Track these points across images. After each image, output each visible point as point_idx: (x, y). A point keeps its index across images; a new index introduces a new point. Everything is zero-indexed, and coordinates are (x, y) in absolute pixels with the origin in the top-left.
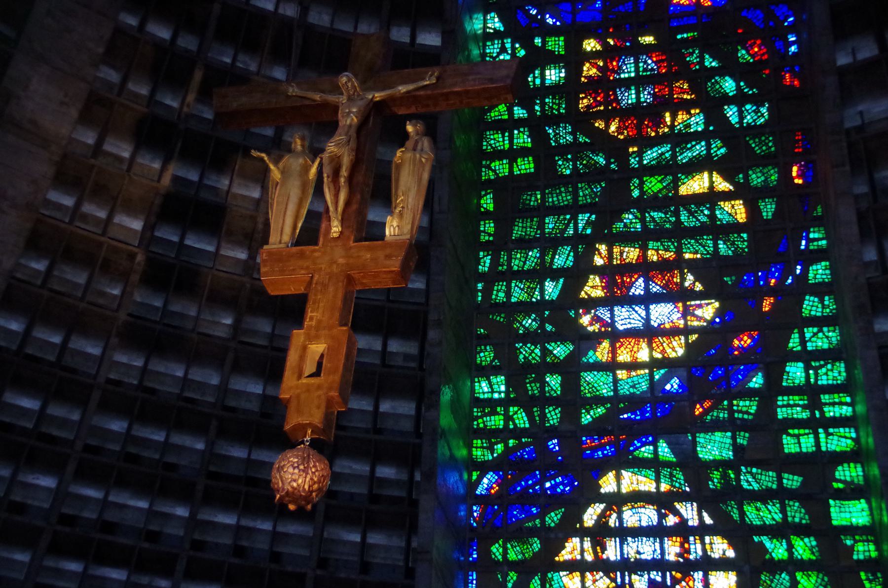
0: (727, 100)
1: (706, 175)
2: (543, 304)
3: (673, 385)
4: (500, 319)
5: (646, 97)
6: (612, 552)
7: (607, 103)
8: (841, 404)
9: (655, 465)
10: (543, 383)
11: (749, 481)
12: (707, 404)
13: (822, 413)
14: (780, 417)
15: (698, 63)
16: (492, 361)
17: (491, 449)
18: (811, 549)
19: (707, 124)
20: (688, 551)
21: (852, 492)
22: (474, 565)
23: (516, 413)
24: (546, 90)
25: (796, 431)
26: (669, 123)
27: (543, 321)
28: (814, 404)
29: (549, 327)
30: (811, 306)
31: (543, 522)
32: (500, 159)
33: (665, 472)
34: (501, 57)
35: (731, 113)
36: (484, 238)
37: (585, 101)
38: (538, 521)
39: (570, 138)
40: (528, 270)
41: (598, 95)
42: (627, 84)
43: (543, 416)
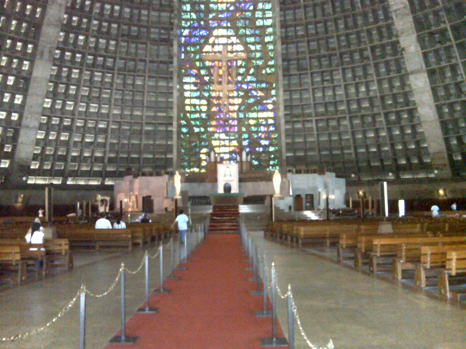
3: (232, 8)
9: (227, 28)
10: (200, 7)
12: (240, 13)
21: (270, 35)
22: (183, 52)
33: (229, 30)
43: (200, 16)
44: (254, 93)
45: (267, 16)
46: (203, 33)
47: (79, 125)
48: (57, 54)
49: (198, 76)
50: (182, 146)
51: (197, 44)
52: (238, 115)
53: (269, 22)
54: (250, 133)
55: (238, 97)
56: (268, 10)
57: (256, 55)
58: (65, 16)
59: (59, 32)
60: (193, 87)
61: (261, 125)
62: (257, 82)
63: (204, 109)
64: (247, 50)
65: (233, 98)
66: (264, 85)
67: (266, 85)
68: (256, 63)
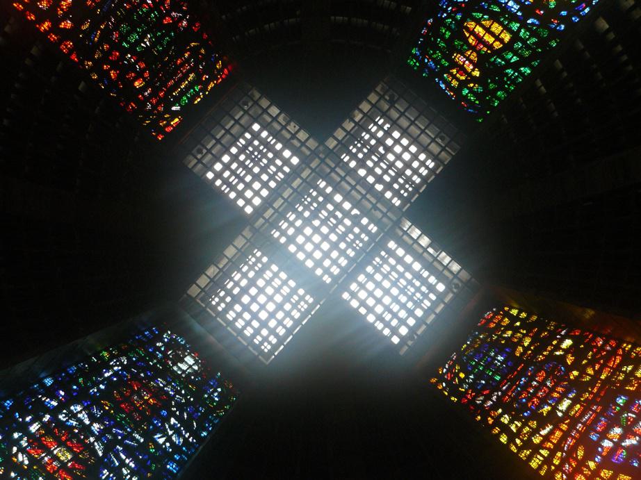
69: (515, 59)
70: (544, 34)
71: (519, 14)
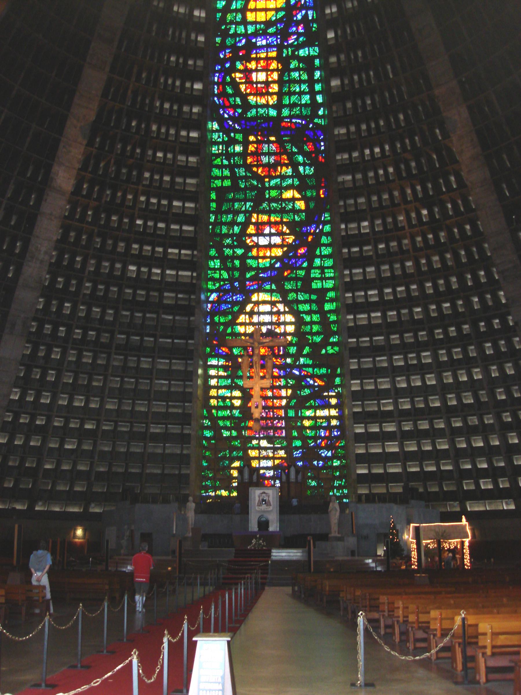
0: (300, 164)
1: (292, 191)
2: (233, 235)
3: (278, 265)
4: (218, 239)
5: (272, 160)
6: (255, 319)
7: (257, 161)
8: (330, 272)
9: (271, 291)
10: (233, 263)
11: (301, 297)
12: (289, 272)
13: (325, 276)
14: (312, 277)
15: (290, 149)
16: (215, 255)
17: (214, 285)
18: (318, 318)
19: (293, 173)
20: (280, 319)
21: (332, 300)
22: (208, 324)
23: (223, 273)
24: (235, 154)
25: (316, 281)
26: (279, 171)
27: (233, 241)
28: (323, 273)
29: (235, 243)
30: (324, 240)
31: (232, 310)
32: (218, 179)
33: (274, 294)
34: (218, 140)
35: (301, 169)
36: (212, 209)
37: (250, 160)
38: (230, 310)
39: (244, 174)
40: (228, 222)
41: (254, 158)
42: (265, 154)
43: (233, 274)
44: (311, 382)
45: (327, 275)
46: (239, 298)
47: (56, 424)
48: (33, 326)
49: (229, 357)
50: (205, 458)
51: (229, 313)
52: (286, 413)
53: (330, 284)
54: (304, 439)
55: (286, 387)
56: (328, 268)
57: (312, 328)
58: (47, 276)
59: (38, 298)
60: (222, 373)
61: (321, 427)
62: (313, 366)
63: (237, 403)
64: (299, 322)
65: (280, 388)
66: (324, 371)
67: (327, 371)
68: (312, 339)
69: (233, 7)
70: (229, 41)
71: (254, 40)
